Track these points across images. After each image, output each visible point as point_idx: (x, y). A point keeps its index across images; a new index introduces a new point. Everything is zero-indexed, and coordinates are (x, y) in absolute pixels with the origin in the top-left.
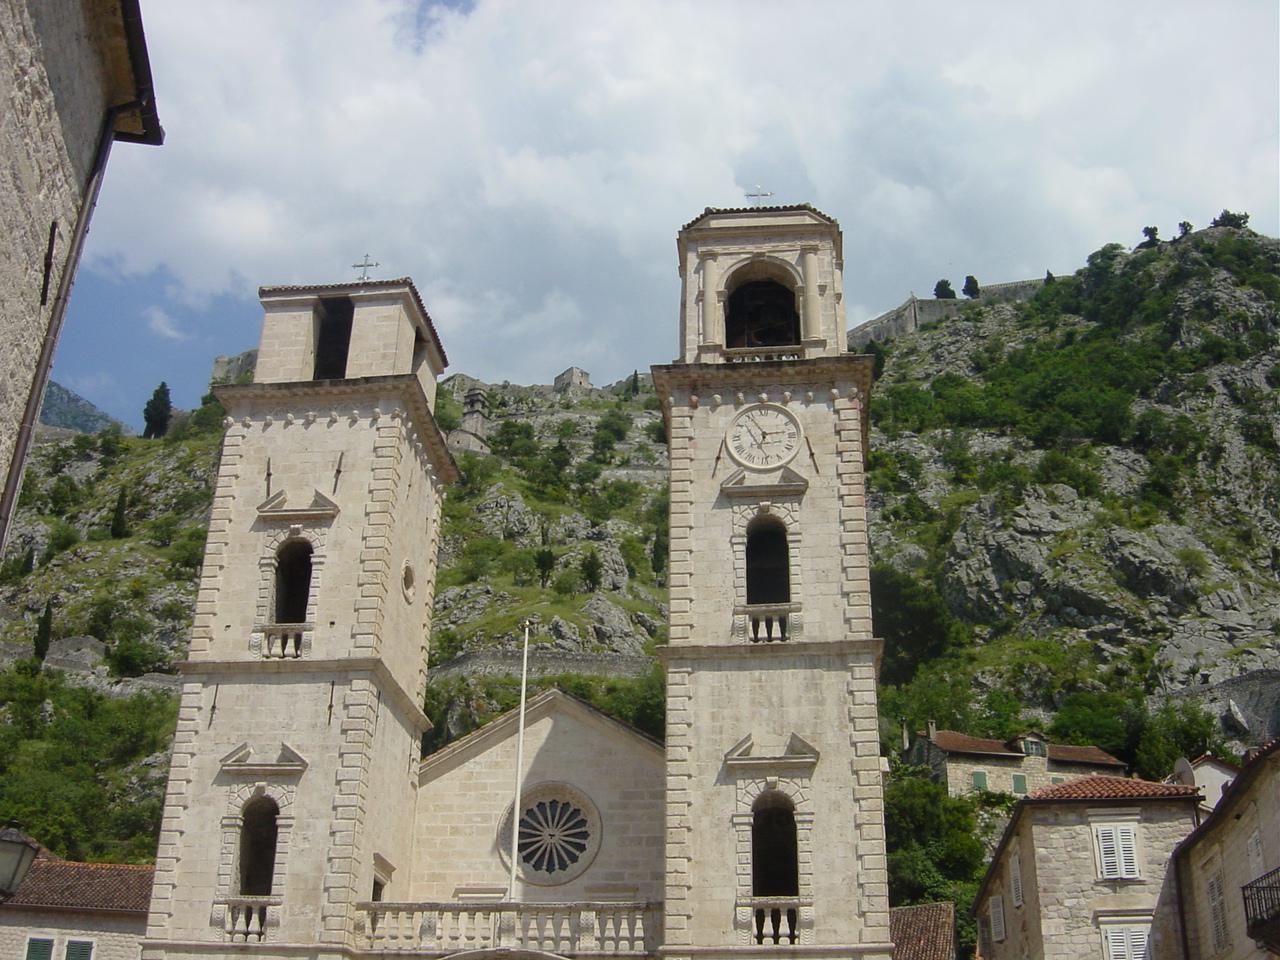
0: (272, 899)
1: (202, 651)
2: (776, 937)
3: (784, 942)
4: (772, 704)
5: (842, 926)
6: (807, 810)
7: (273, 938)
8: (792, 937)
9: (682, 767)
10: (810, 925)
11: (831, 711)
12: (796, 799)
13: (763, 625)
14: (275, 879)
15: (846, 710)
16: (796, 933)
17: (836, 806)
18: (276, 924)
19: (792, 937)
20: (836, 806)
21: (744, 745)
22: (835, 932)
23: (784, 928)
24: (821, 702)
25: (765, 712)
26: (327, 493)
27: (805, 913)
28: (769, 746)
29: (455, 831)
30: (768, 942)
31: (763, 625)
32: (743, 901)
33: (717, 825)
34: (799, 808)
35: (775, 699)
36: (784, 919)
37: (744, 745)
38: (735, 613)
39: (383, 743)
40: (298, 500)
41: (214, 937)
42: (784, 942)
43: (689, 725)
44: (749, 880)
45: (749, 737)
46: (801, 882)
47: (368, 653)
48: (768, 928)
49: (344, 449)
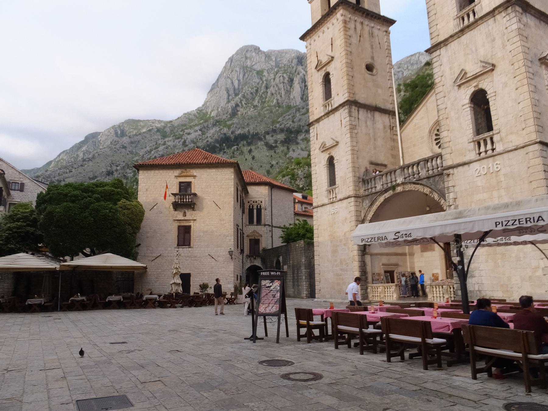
0: (336, 186)
1: (312, 119)
2: (486, 152)
3: (490, 152)
4: (473, 52)
5: (513, 137)
6: (492, 91)
7: (339, 197)
8: (493, 150)
9: (442, 95)
10: (498, 142)
11: (498, 42)
12: (486, 89)
13: (466, 19)
14: (337, 180)
15: (505, 38)
16: (494, 147)
17: (505, 85)
18: (339, 193)
19: (493, 150)
20: (505, 85)
21: (463, 73)
22: (512, 142)
23: (489, 146)
24: (494, 40)
25: (470, 57)
26: (330, 53)
27: (495, 139)
28: (472, 69)
29: (414, 145)
30: (483, 155)
31: (466, 19)
32: (470, 141)
33: (457, 113)
34: (488, 92)
35: (474, 49)
36: (489, 142)
37: (463, 73)
38: (454, 20)
39: (367, 126)
40: (324, 60)
41: (326, 201)
42: (490, 152)
43: (442, 76)
44: (471, 131)
45: (462, 70)
46: (493, 124)
47: (346, 99)
48: (482, 149)
49: (331, 36)
